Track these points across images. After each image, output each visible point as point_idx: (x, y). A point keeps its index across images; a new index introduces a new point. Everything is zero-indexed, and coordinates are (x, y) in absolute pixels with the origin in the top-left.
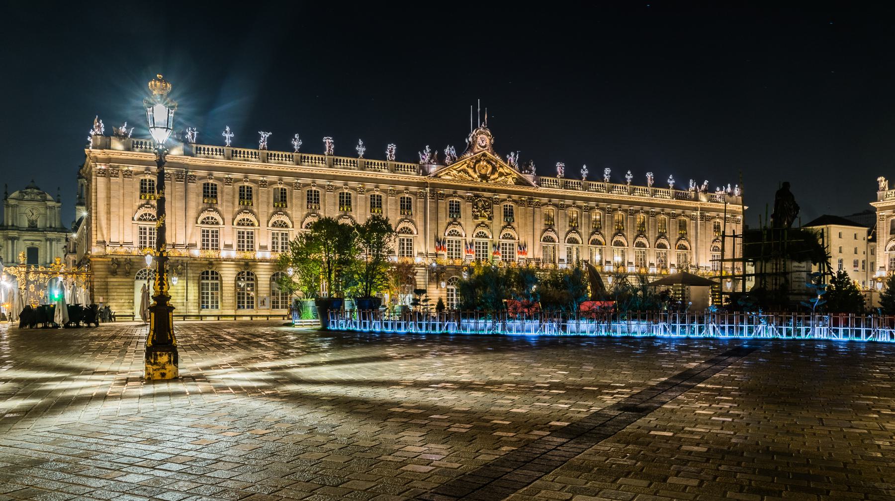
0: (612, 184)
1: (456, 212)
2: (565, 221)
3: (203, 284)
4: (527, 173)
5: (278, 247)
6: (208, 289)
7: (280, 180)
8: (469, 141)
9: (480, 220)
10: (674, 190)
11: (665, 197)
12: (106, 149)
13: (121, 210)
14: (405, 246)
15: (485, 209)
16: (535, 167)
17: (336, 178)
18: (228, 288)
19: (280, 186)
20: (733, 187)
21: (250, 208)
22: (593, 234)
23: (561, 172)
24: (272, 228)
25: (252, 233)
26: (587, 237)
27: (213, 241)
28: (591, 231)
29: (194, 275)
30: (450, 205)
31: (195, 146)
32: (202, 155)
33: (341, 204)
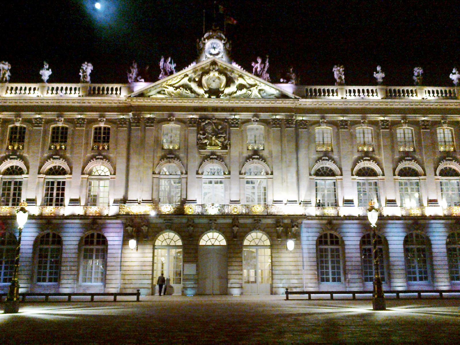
4: (283, 83)
23: (340, 78)
26: (391, 166)
28: (397, 157)
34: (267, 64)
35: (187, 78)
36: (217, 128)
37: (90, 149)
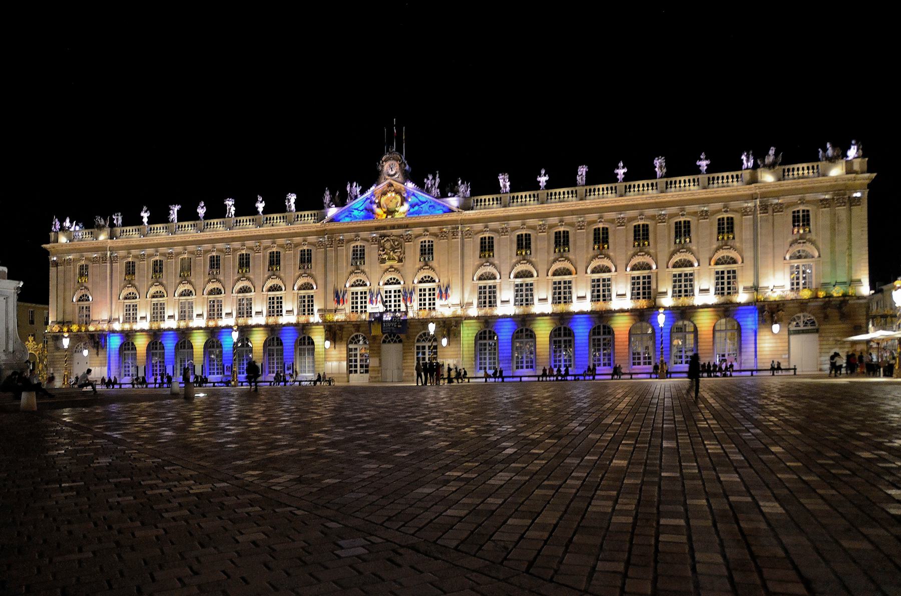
1: (360, 258)
2: (511, 250)
4: (451, 196)
9: (388, 263)
14: (306, 303)
15: (393, 250)
17: (234, 239)
21: (160, 280)
30: (354, 251)
34: (438, 180)
36: (394, 243)
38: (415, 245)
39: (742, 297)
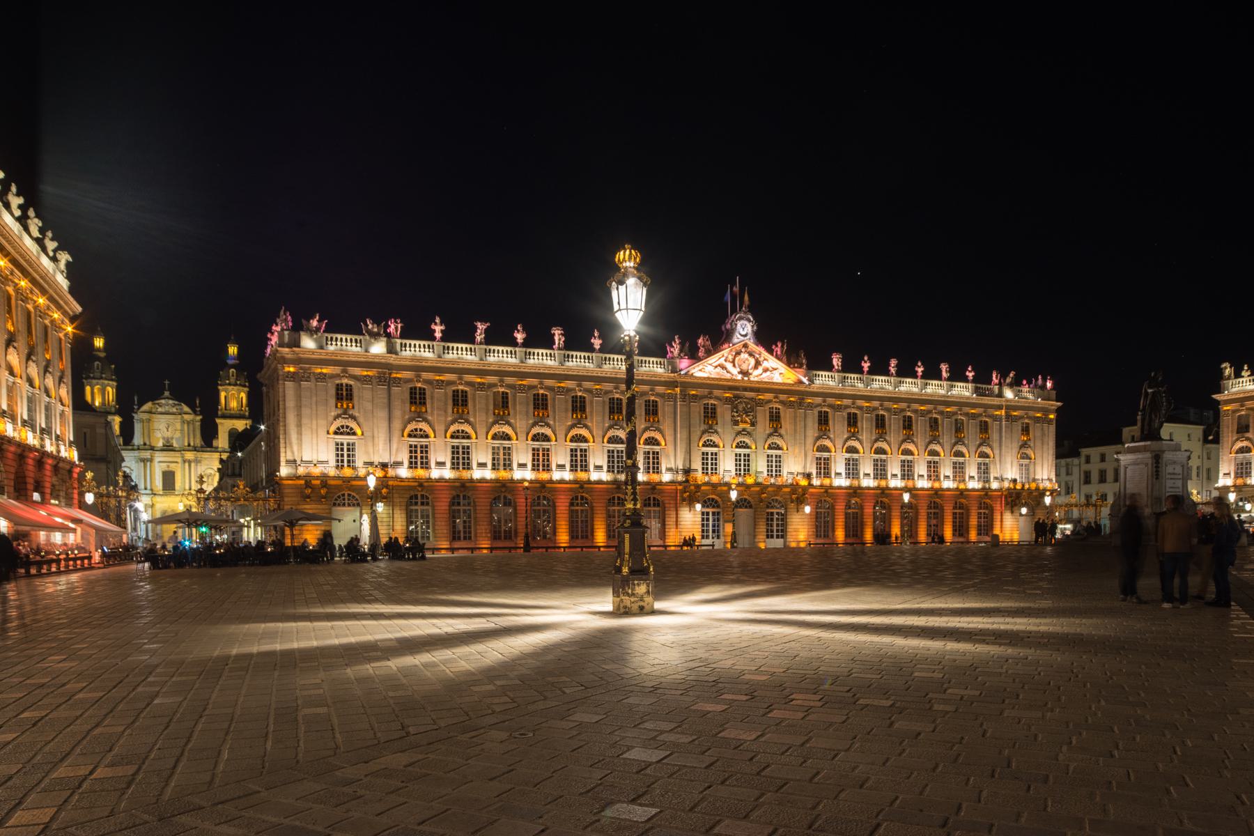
0: (899, 379)
3: (412, 510)
5: (499, 464)
6: (417, 517)
7: (502, 381)
8: (726, 329)
9: (742, 426)
10: (974, 385)
11: (963, 391)
12: (295, 347)
13: (314, 422)
14: (651, 461)
15: (746, 413)
16: (807, 359)
18: (441, 516)
19: (501, 390)
20: (1045, 380)
21: (465, 417)
22: (876, 440)
24: (492, 441)
25: (468, 447)
26: (869, 445)
27: (422, 458)
28: (874, 438)
29: (401, 500)
30: (705, 408)
31: (399, 341)
32: (408, 352)
33: (574, 410)
35: (724, 358)
37: (643, 420)
38: (765, 410)
39: (995, 485)
